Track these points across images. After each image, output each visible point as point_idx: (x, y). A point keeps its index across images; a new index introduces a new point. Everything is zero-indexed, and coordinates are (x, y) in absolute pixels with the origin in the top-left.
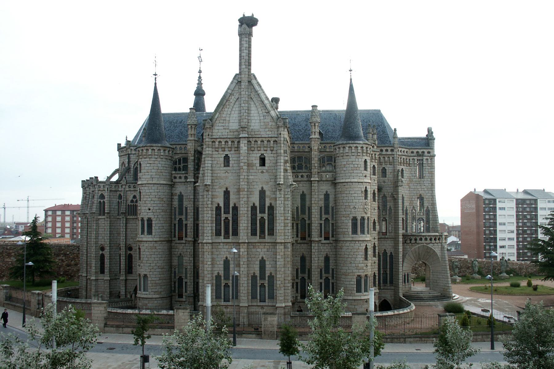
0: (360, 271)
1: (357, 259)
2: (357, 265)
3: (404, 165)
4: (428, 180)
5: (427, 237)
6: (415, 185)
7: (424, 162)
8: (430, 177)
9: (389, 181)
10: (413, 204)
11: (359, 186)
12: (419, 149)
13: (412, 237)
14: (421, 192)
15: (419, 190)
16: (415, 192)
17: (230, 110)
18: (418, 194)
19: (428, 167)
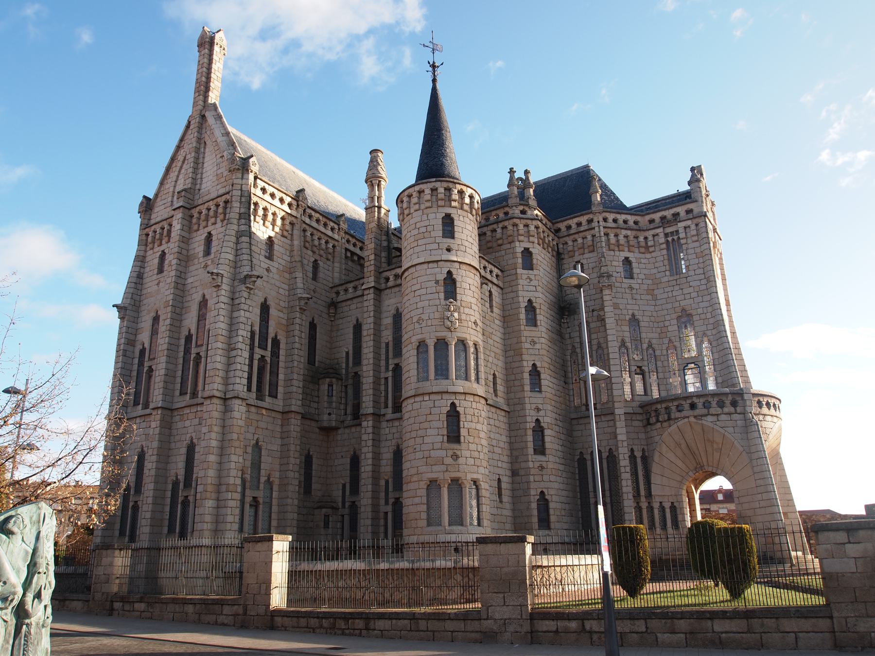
0: (435, 468)
1: (427, 440)
2: (426, 454)
3: (629, 251)
4: (698, 272)
5: (695, 400)
6: (666, 290)
7: (682, 235)
8: (701, 265)
9: (592, 286)
10: (669, 335)
11: (429, 272)
12: (665, 210)
13: (659, 406)
14: (683, 303)
15: (678, 298)
16: (669, 306)
17: (176, 173)
18: (679, 310)
19: (691, 245)
